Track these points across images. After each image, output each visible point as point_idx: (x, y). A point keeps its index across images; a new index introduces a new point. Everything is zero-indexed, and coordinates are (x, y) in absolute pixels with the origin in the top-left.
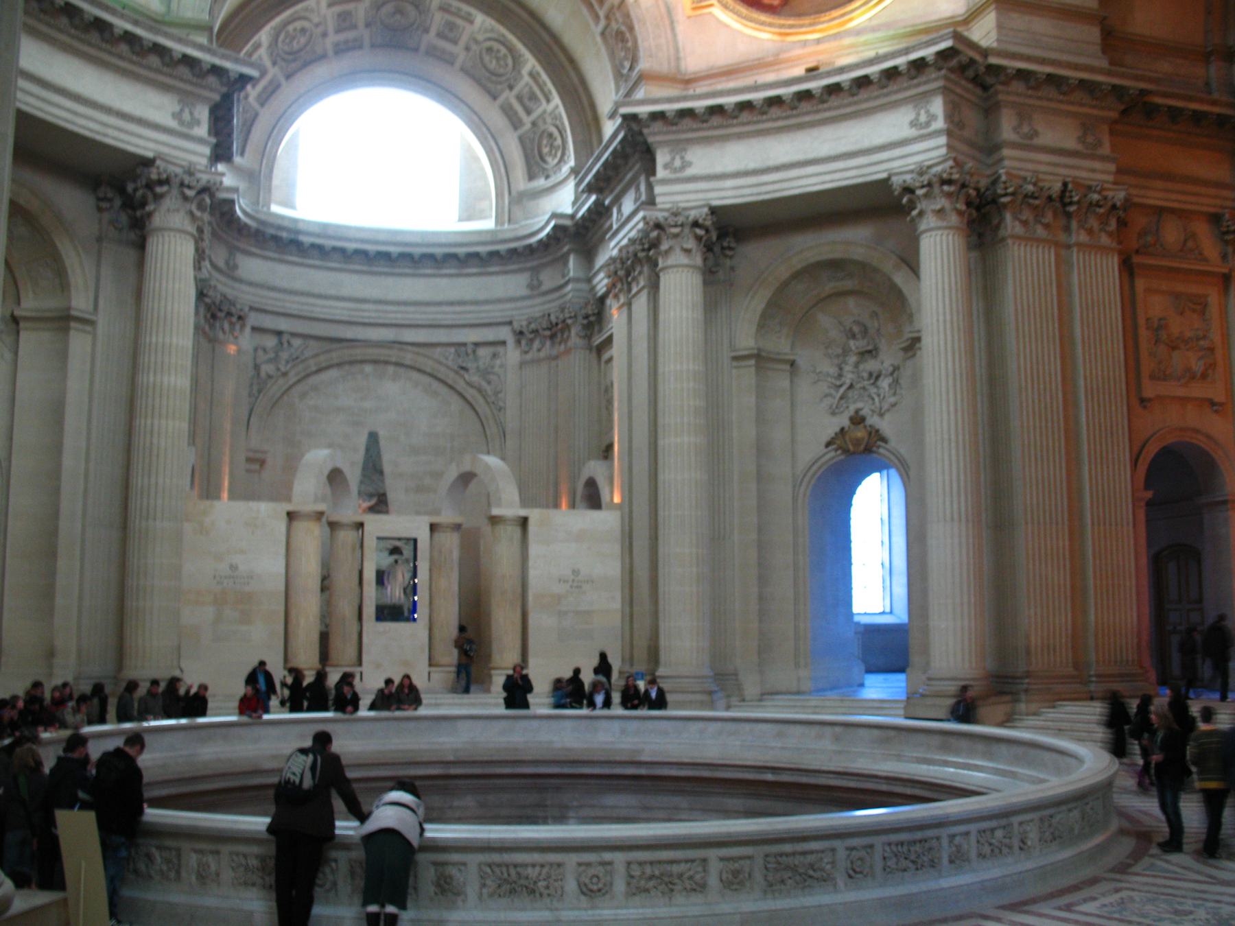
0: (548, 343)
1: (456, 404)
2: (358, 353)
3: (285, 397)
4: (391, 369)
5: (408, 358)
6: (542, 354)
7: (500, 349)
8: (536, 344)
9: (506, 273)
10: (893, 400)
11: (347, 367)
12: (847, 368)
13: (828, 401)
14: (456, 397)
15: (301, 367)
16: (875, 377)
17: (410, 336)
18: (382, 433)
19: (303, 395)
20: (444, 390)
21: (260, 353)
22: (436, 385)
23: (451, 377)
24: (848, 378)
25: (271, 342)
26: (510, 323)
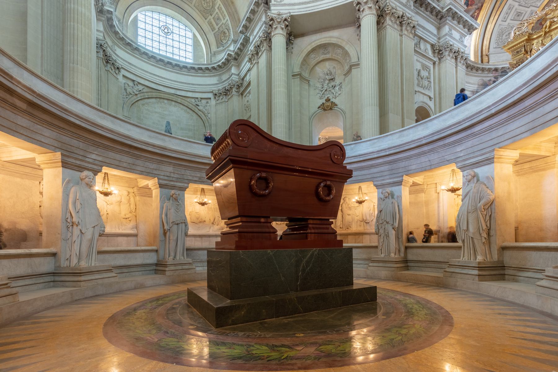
0: (225, 97)
1: (195, 116)
2: (162, 95)
3: (136, 103)
4: (173, 103)
5: (179, 100)
6: (223, 100)
7: (209, 101)
8: (221, 97)
9: (210, 76)
10: (339, 92)
11: (158, 99)
12: (325, 85)
13: (319, 95)
14: (195, 114)
15: (142, 95)
16: (334, 87)
17: (179, 93)
18: (171, 122)
19: (143, 105)
20: (191, 112)
21: (126, 85)
22: (188, 110)
23: (194, 108)
24: (326, 87)
25: (131, 84)
26: (212, 92)
